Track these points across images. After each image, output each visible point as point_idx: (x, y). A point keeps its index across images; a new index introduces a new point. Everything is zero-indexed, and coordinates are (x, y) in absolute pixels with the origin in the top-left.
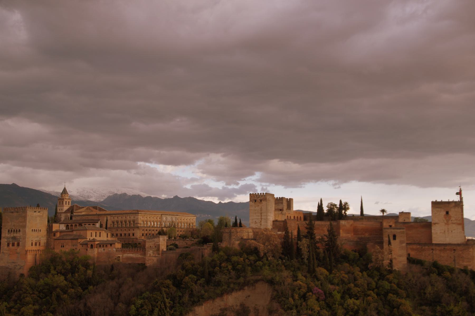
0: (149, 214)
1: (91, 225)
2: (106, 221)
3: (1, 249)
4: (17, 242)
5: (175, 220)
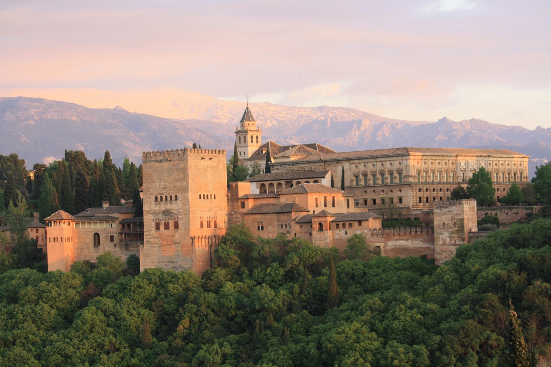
0: (431, 156)
1: (311, 184)
2: (341, 174)
3: (145, 236)
4: (173, 221)
5: (464, 167)
